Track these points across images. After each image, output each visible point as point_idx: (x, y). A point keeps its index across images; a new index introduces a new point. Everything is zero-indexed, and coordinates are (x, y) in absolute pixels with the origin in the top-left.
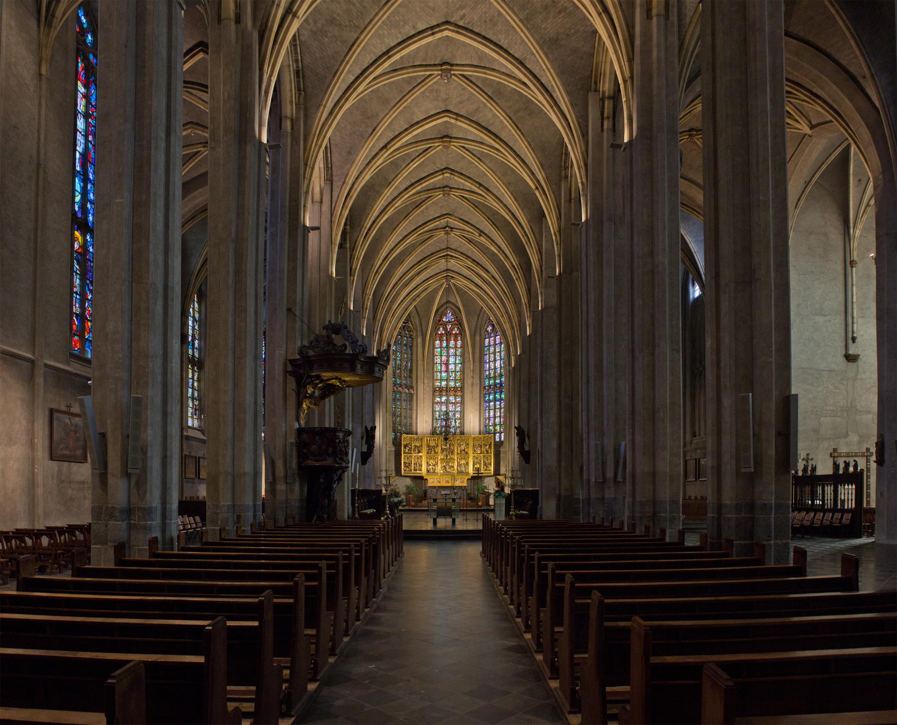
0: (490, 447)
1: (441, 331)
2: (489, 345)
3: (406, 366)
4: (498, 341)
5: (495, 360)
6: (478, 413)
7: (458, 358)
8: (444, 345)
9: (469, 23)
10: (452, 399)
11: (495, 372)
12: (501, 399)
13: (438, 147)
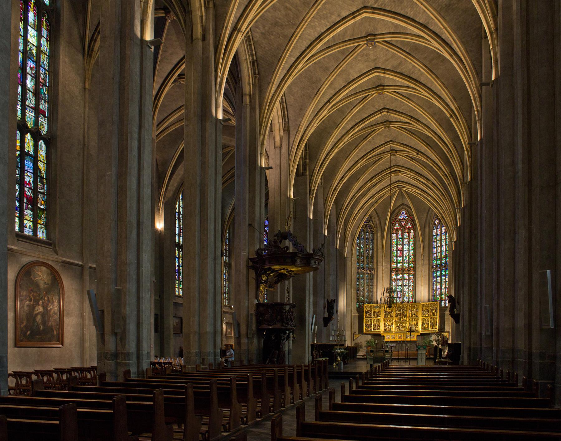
1: (397, 226)
2: (437, 235)
3: (369, 254)
4: (443, 231)
5: (441, 246)
6: (427, 286)
7: (411, 246)
8: (400, 236)
9: (381, 5)
10: (406, 276)
11: (441, 255)
12: (446, 275)
13: (374, 94)
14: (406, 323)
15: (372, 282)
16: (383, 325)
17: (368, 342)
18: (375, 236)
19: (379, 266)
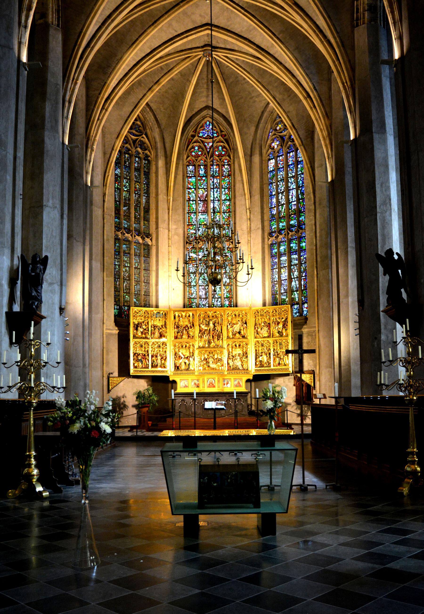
0: (285, 326)
2: (277, 168)
8: (202, 172)
14: (221, 353)
15: (148, 263)
16: (173, 357)
17: (139, 396)
18: (153, 168)
19: (160, 229)
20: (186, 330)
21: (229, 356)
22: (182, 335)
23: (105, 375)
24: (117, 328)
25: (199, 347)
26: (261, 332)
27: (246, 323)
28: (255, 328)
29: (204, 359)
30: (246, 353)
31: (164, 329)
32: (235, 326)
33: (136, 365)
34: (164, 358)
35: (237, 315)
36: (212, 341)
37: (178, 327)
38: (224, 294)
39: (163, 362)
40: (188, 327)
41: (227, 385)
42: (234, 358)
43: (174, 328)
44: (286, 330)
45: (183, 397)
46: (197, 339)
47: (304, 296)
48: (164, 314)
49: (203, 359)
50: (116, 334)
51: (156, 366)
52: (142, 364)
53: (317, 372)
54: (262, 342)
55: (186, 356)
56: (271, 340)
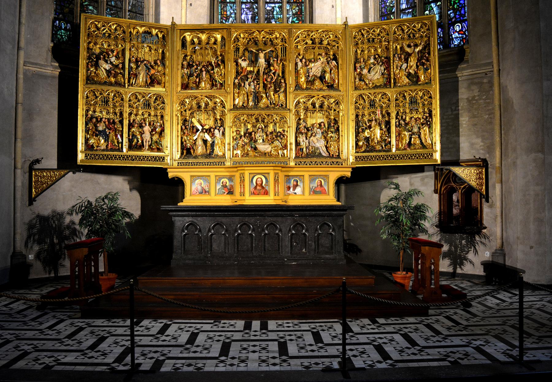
0: (423, 59)
20: (208, 71)
21: (298, 129)
22: (199, 82)
23: (19, 165)
24: (57, 64)
25: (235, 107)
26: (369, 76)
27: (335, 59)
28: (355, 69)
29: (245, 134)
30: (336, 122)
31: (160, 69)
32: (312, 65)
33: (92, 141)
34: (158, 130)
35: (317, 40)
36: (264, 95)
37: (190, 66)
38: (288, 18)
39: (155, 137)
40: (212, 65)
41: (294, 189)
42: (310, 133)
43: (183, 67)
44: (426, 69)
45: (192, 216)
46: (230, 89)
47: (453, 9)
48: (160, 36)
49: (242, 134)
50: (53, 77)
51: (140, 147)
52: (106, 140)
53: (495, 160)
54: (372, 98)
55: (207, 127)
56: (391, 93)
